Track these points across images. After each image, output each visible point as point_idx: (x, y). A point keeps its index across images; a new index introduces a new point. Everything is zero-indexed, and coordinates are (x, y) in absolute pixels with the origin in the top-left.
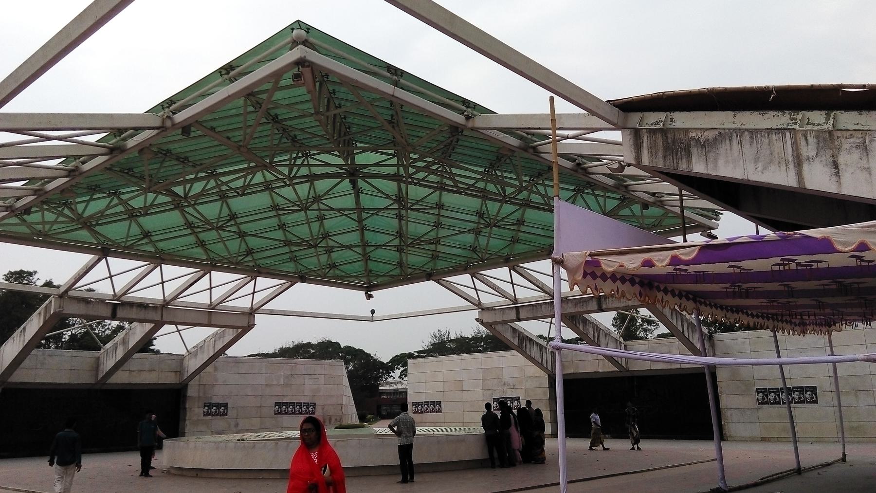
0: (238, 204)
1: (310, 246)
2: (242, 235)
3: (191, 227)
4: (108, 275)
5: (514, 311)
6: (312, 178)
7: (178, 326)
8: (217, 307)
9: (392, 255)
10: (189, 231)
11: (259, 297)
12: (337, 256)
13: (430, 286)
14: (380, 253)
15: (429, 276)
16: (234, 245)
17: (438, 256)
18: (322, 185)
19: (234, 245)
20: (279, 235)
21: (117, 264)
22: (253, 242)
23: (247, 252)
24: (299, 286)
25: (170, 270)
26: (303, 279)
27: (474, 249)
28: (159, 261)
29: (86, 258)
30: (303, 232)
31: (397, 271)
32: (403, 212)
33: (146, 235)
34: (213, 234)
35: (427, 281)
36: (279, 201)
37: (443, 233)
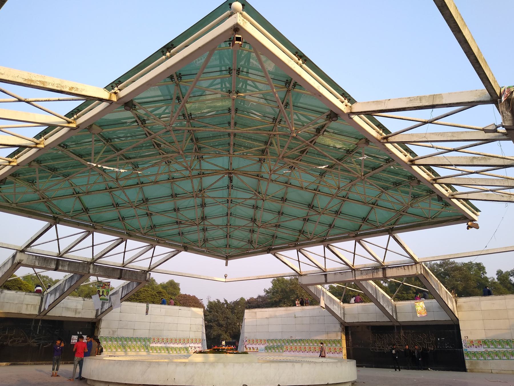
0: (151, 191)
1: (194, 224)
2: (149, 215)
3: (117, 206)
4: (57, 238)
5: (324, 276)
6: (202, 174)
7: (98, 277)
8: (127, 266)
9: (246, 235)
10: (115, 208)
11: (155, 260)
12: (211, 234)
13: (269, 256)
14: (237, 233)
15: (269, 250)
16: (145, 222)
17: (276, 237)
18: (207, 181)
19: (145, 222)
20: (174, 214)
21: (63, 230)
22: (158, 219)
23: (151, 227)
24: (183, 254)
25: (100, 237)
26: (186, 249)
27: (301, 232)
28: (91, 230)
29: (42, 224)
30: (190, 214)
31: (248, 246)
32: (260, 203)
33: (86, 210)
34: (131, 212)
35: (268, 253)
36: (178, 190)
37: (283, 218)
